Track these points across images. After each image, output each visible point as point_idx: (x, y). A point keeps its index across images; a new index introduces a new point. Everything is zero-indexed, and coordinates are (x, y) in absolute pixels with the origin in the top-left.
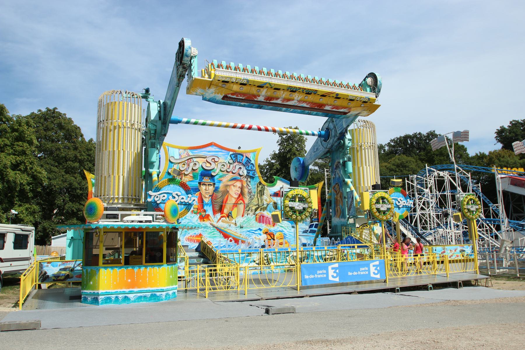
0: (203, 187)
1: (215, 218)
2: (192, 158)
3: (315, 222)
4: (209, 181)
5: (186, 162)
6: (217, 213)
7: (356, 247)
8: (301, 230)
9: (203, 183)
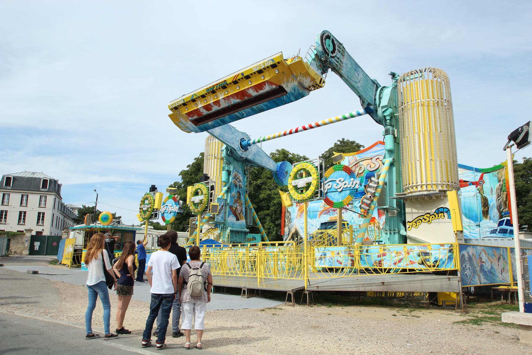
1: (381, 221)
2: (358, 163)
3: (506, 217)
5: (354, 167)
6: (382, 216)
7: (277, 245)
8: (487, 229)
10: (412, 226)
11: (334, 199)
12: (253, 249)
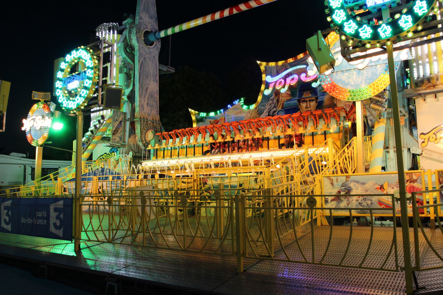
0: (304, 105)
4: (311, 95)
9: (303, 99)
10: (429, 139)
11: (347, 84)
12: (183, 182)
